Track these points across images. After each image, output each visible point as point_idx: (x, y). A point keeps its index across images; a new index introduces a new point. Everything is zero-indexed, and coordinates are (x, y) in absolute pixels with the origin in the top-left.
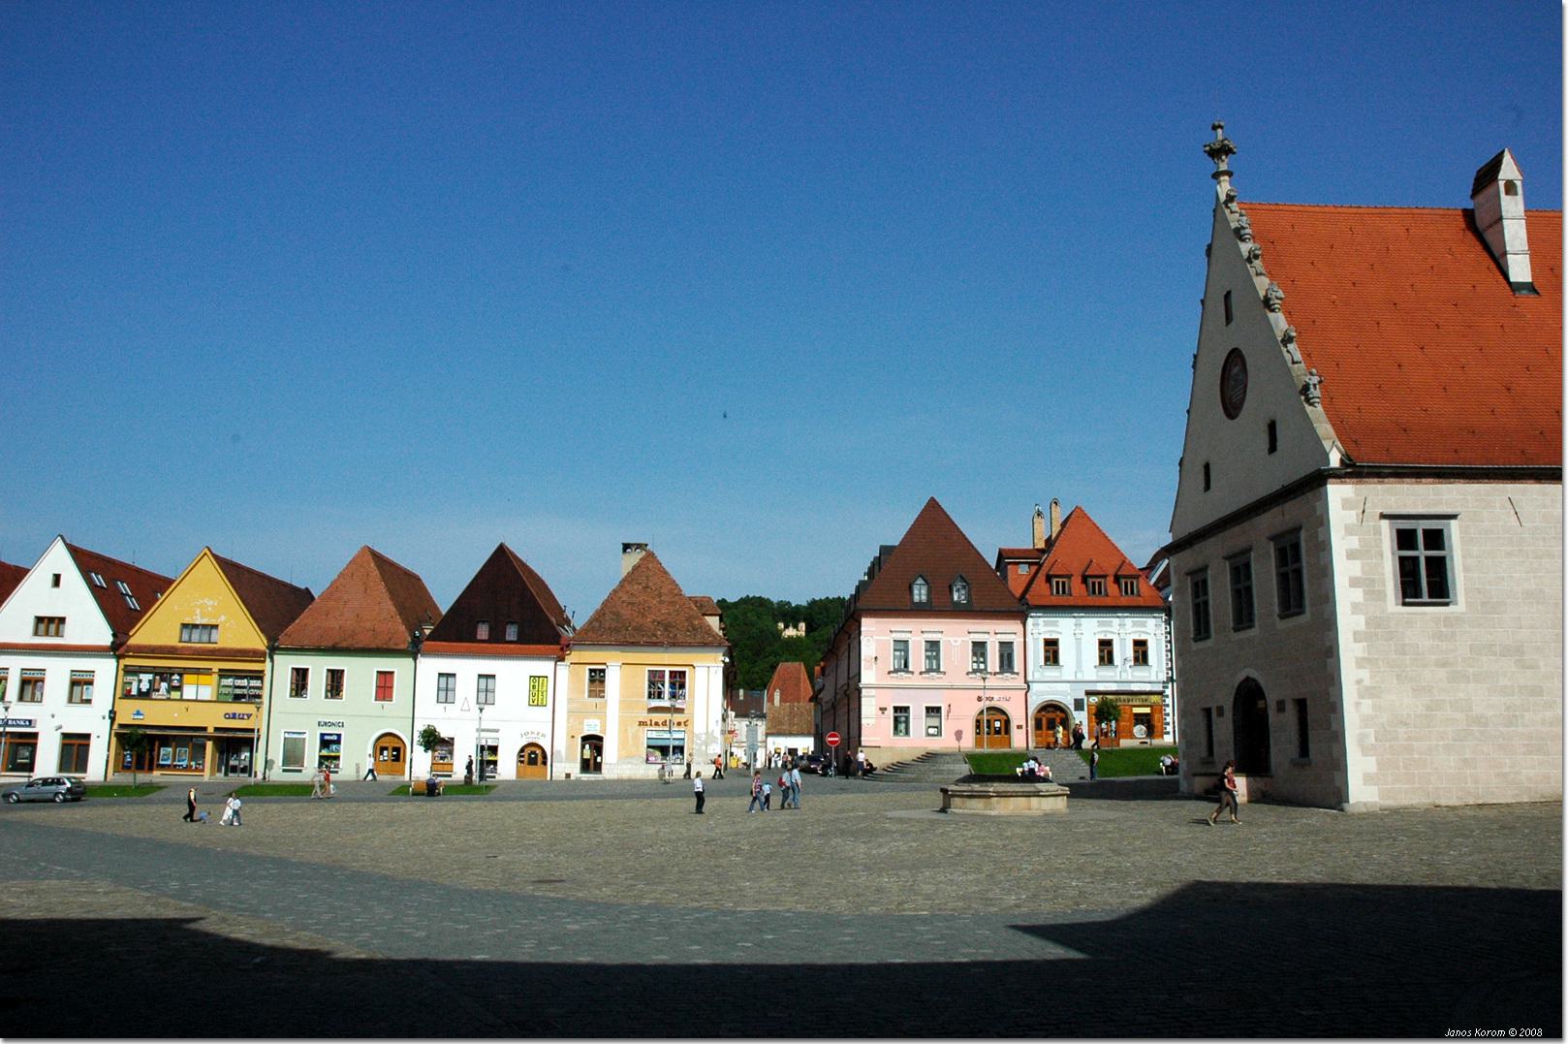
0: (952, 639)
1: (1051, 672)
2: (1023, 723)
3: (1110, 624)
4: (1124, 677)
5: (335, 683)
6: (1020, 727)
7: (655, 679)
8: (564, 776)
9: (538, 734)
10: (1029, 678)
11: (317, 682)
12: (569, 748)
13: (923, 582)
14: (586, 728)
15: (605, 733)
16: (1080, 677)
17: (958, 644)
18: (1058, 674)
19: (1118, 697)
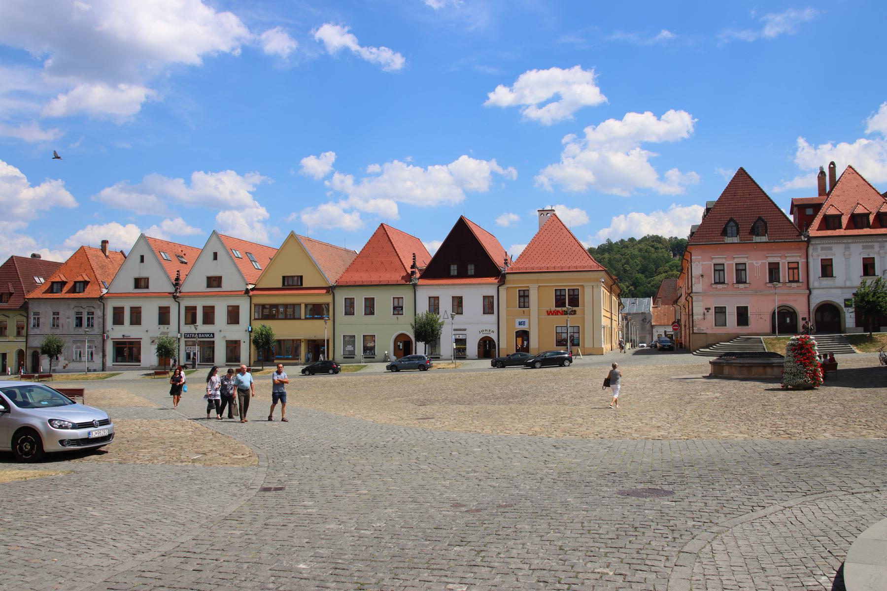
0: (754, 262)
1: (827, 282)
2: (806, 316)
3: (872, 247)
5: (370, 307)
6: (803, 319)
9: (489, 331)
10: (811, 286)
11: (360, 306)
13: (734, 225)
16: (848, 284)
17: (760, 264)
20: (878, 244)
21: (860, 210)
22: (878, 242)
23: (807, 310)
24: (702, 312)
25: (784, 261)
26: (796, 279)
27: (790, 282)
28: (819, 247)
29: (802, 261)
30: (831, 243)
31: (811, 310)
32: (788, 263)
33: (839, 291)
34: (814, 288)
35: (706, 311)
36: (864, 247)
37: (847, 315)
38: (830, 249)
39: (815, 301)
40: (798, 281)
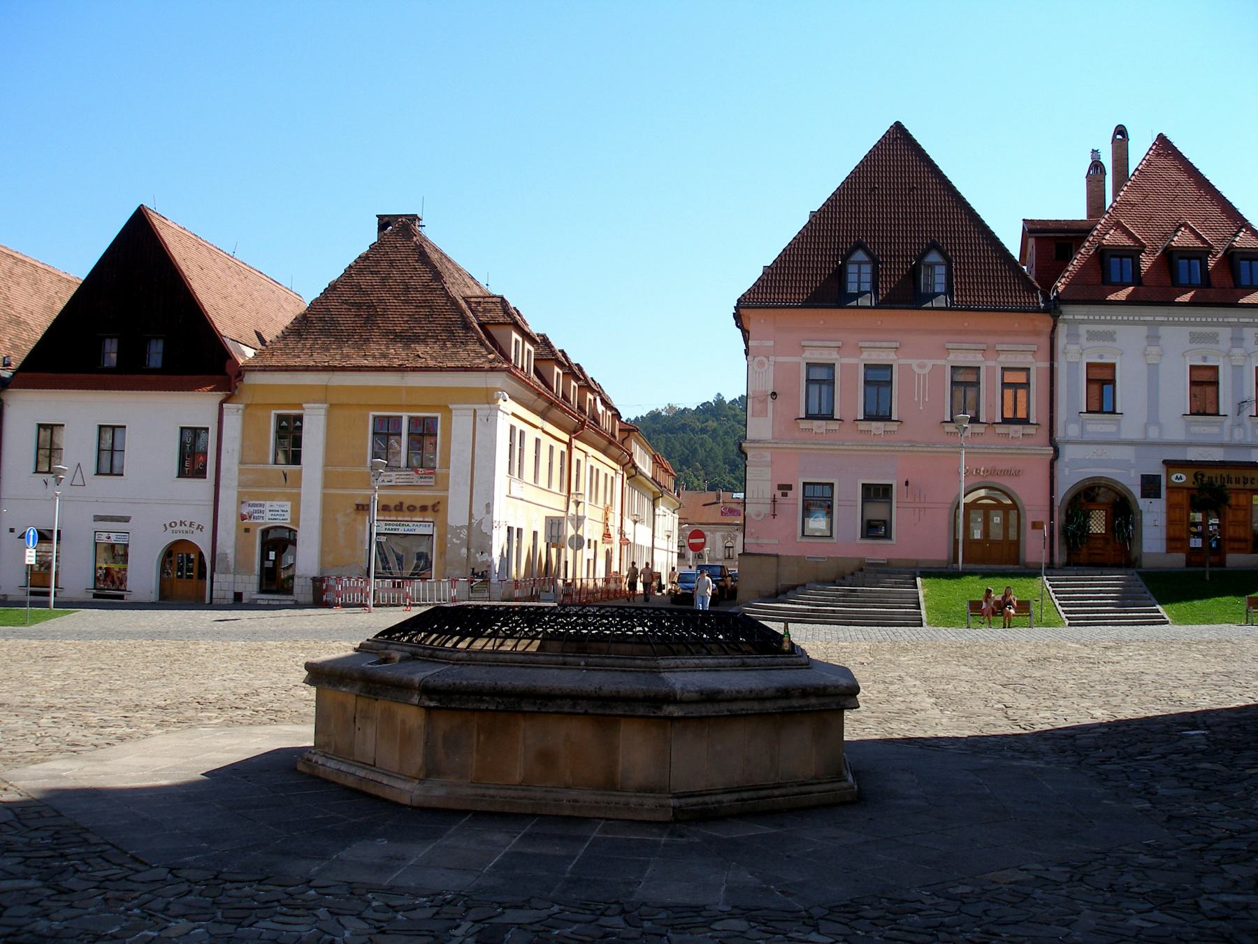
0: (914, 363)
1: (1099, 426)
2: (1043, 517)
3: (1213, 338)
4: (1238, 436)
7: (385, 430)
8: (232, 596)
9: (191, 524)
10: (1059, 435)
12: (238, 549)
13: (865, 258)
14: (268, 515)
15: (298, 525)
16: (1153, 434)
17: (926, 371)
18: (1113, 428)
19: (1224, 472)
20: (1229, 329)
21: (1182, 239)
22: (1229, 324)
23: (1048, 503)
24: (769, 496)
25: (991, 363)
26: (1021, 414)
27: (1006, 421)
28: (1083, 329)
29: (1039, 365)
30: (1111, 322)
31: (1057, 502)
32: (1004, 369)
33: (1128, 453)
34: (1068, 442)
35: (778, 494)
36: (1194, 338)
37: (1147, 520)
38: (1110, 336)
39: (1068, 479)
40: (1025, 421)
